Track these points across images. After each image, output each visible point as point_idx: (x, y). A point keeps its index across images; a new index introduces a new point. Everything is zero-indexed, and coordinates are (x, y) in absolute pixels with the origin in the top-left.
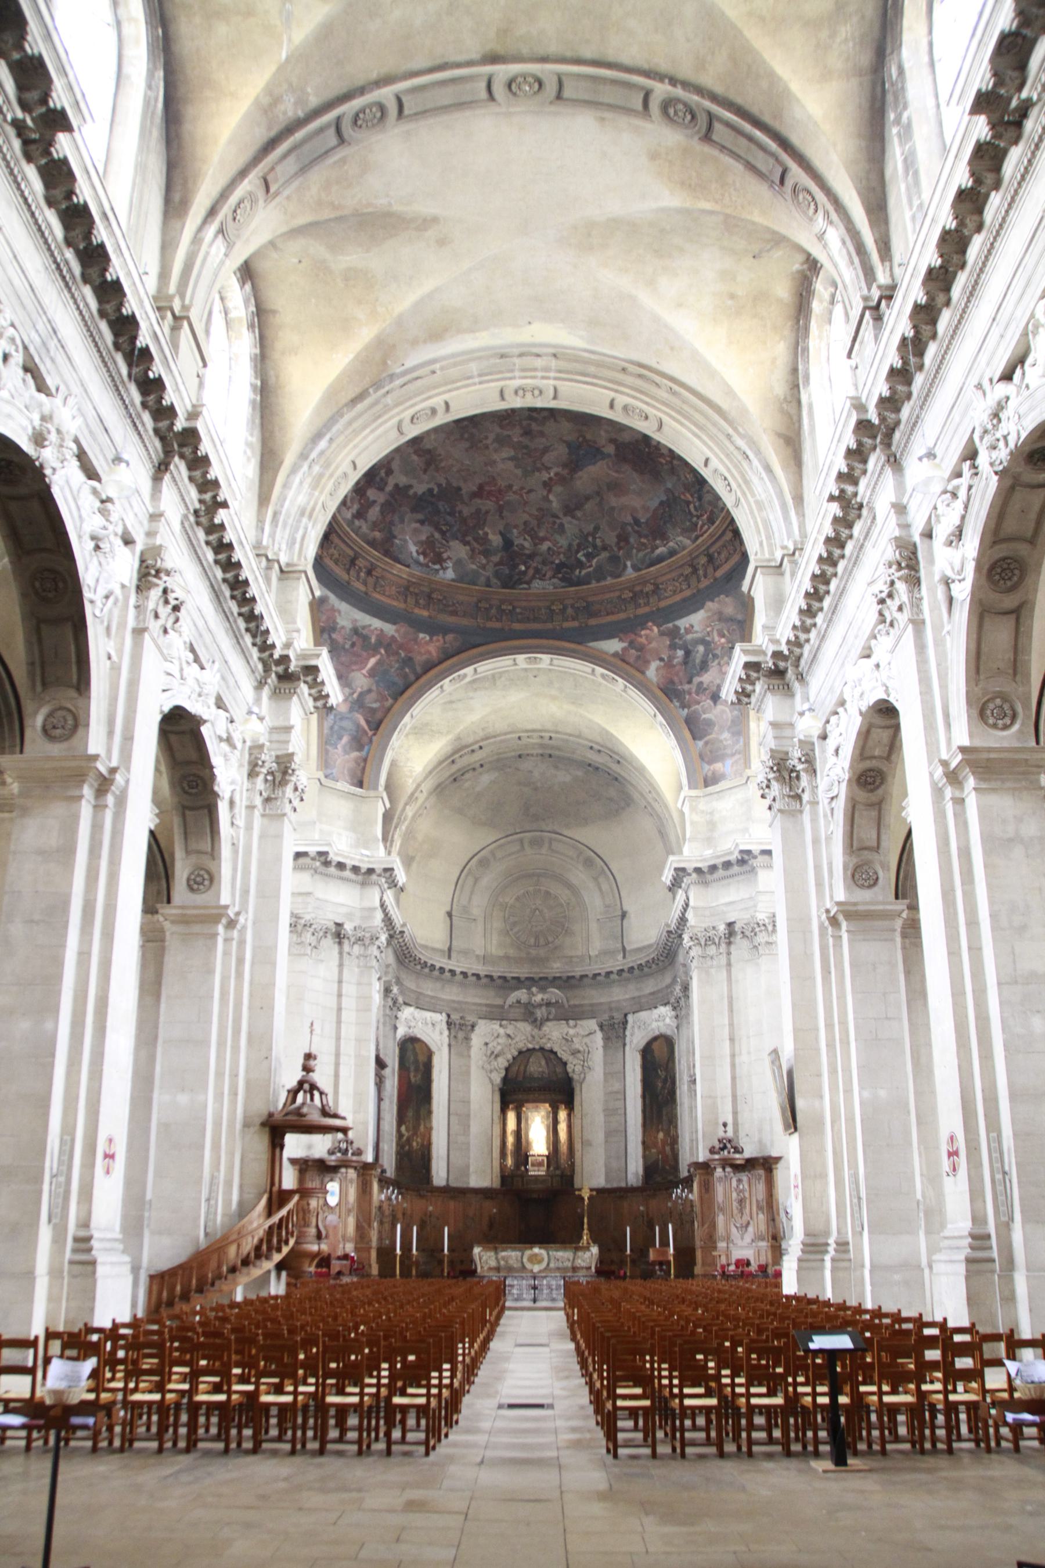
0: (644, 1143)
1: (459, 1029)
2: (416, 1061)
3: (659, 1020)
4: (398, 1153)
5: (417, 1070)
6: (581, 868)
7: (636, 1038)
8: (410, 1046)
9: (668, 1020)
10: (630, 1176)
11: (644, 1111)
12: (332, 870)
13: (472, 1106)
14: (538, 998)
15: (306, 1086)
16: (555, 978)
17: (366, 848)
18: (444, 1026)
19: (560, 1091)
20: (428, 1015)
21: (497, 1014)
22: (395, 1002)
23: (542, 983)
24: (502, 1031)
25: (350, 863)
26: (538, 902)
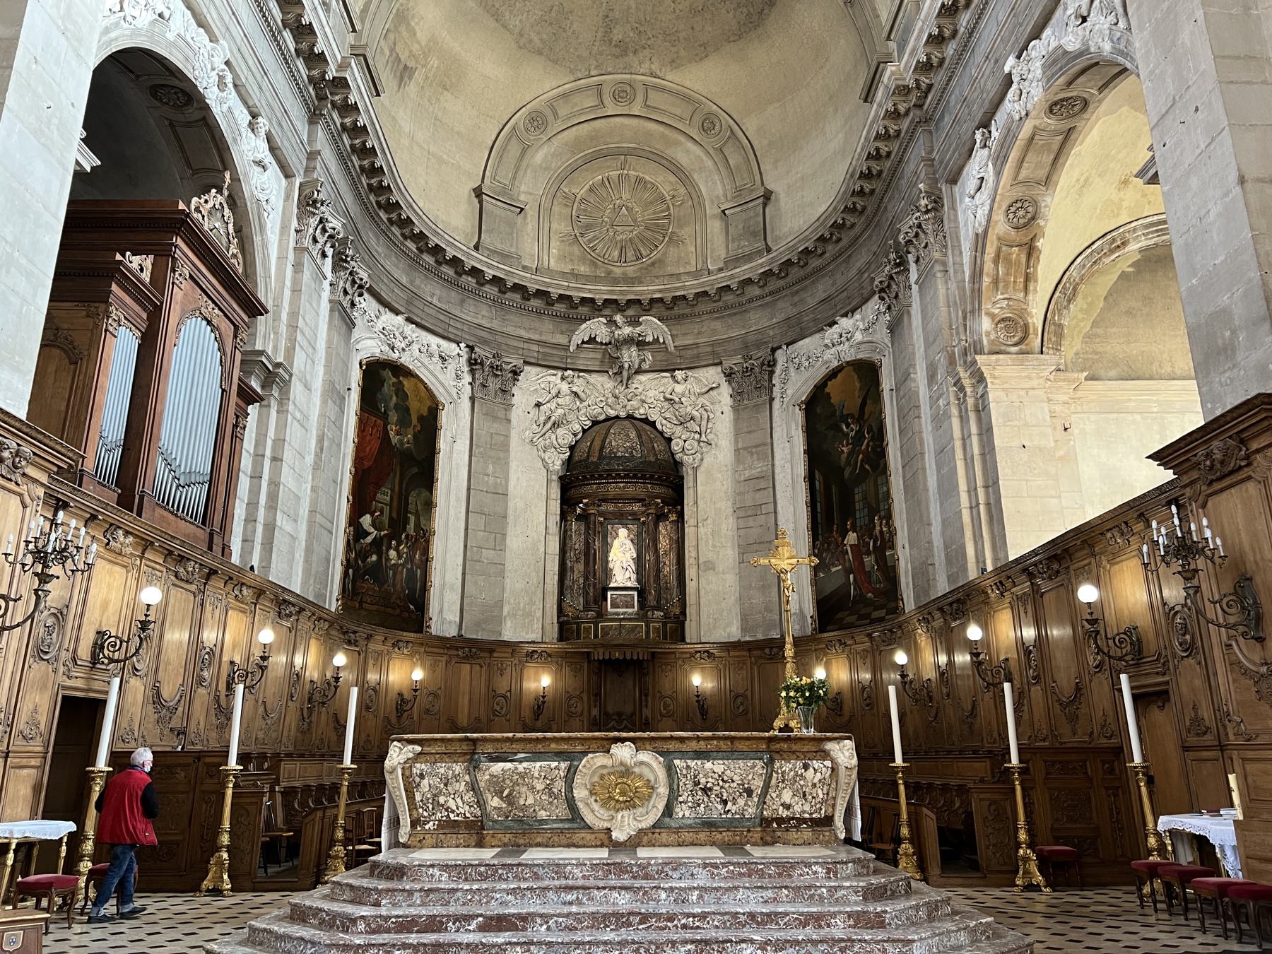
1: (492, 374)
2: (404, 411)
4: (348, 565)
5: (404, 422)
8: (387, 374)
13: (511, 504)
14: (627, 330)
16: (653, 301)
18: (466, 369)
20: (434, 341)
23: (630, 312)
24: (564, 387)
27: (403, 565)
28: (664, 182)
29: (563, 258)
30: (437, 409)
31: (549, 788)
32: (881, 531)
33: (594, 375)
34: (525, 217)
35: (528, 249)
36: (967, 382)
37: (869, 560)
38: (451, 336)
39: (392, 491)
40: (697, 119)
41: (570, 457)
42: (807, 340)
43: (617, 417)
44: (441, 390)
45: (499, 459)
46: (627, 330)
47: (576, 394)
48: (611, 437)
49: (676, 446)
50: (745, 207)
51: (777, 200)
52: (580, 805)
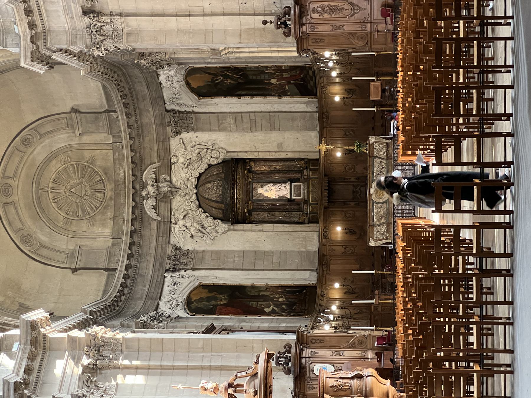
0: (280, 96)
1: (180, 261)
2: (208, 299)
3: (170, 80)
4: (289, 315)
5: (216, 299)
6: (30, 150)
7: (188, 101)
9: (172, 73)
10: (309, 110)
11: (253, 96)
12: (33, 378)
13: (248, 249)
15: (231, 391)
17: (12, 346)
18: (178, 273)
19: (235, 171)
20: (166, 289)
21: (166, 225)
22: (154, 318)
23: (137, 187)
24: (181, 223)
25: (24, 363)
26: (63, 189)
27: (285, 296)
28: (55, 166)
29: (104, 225)
30: (202, 286)
31: (380, 208)
32: (273, 70)
33: (173, 207)
34: (83, 246)
35: (103, 243)
36: (227, 51)
37: (285, 75)
38: (162, 280)
39: (250, 301)
40: (22, 148)
41: (219, 219)
42: (165, 95)
43: (196, 194)
44: (192, 284)
45: (225, 256)
46: (150, 188)
47: (184, 217)
48: (210, 197)
49: (214, 162)
50: (79, 123)
51: (78, 106)
52: (384, 200)
